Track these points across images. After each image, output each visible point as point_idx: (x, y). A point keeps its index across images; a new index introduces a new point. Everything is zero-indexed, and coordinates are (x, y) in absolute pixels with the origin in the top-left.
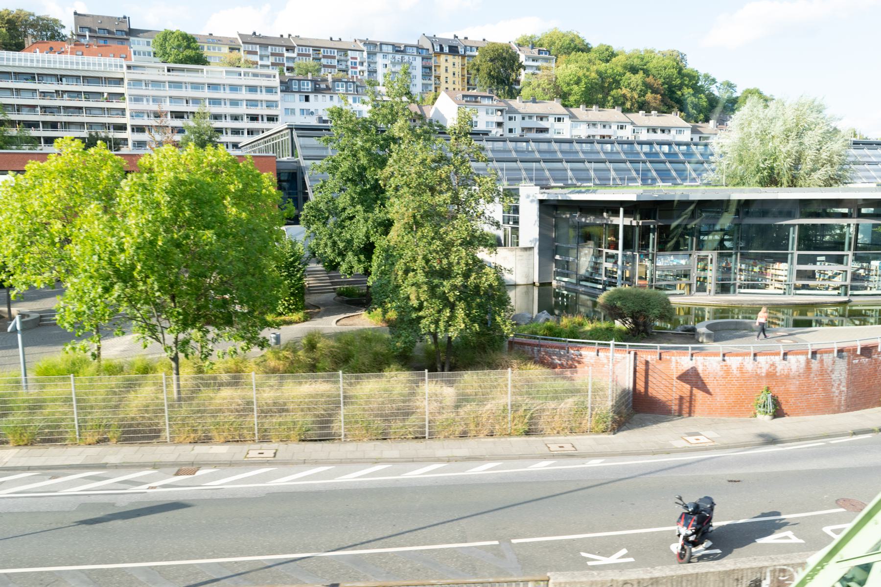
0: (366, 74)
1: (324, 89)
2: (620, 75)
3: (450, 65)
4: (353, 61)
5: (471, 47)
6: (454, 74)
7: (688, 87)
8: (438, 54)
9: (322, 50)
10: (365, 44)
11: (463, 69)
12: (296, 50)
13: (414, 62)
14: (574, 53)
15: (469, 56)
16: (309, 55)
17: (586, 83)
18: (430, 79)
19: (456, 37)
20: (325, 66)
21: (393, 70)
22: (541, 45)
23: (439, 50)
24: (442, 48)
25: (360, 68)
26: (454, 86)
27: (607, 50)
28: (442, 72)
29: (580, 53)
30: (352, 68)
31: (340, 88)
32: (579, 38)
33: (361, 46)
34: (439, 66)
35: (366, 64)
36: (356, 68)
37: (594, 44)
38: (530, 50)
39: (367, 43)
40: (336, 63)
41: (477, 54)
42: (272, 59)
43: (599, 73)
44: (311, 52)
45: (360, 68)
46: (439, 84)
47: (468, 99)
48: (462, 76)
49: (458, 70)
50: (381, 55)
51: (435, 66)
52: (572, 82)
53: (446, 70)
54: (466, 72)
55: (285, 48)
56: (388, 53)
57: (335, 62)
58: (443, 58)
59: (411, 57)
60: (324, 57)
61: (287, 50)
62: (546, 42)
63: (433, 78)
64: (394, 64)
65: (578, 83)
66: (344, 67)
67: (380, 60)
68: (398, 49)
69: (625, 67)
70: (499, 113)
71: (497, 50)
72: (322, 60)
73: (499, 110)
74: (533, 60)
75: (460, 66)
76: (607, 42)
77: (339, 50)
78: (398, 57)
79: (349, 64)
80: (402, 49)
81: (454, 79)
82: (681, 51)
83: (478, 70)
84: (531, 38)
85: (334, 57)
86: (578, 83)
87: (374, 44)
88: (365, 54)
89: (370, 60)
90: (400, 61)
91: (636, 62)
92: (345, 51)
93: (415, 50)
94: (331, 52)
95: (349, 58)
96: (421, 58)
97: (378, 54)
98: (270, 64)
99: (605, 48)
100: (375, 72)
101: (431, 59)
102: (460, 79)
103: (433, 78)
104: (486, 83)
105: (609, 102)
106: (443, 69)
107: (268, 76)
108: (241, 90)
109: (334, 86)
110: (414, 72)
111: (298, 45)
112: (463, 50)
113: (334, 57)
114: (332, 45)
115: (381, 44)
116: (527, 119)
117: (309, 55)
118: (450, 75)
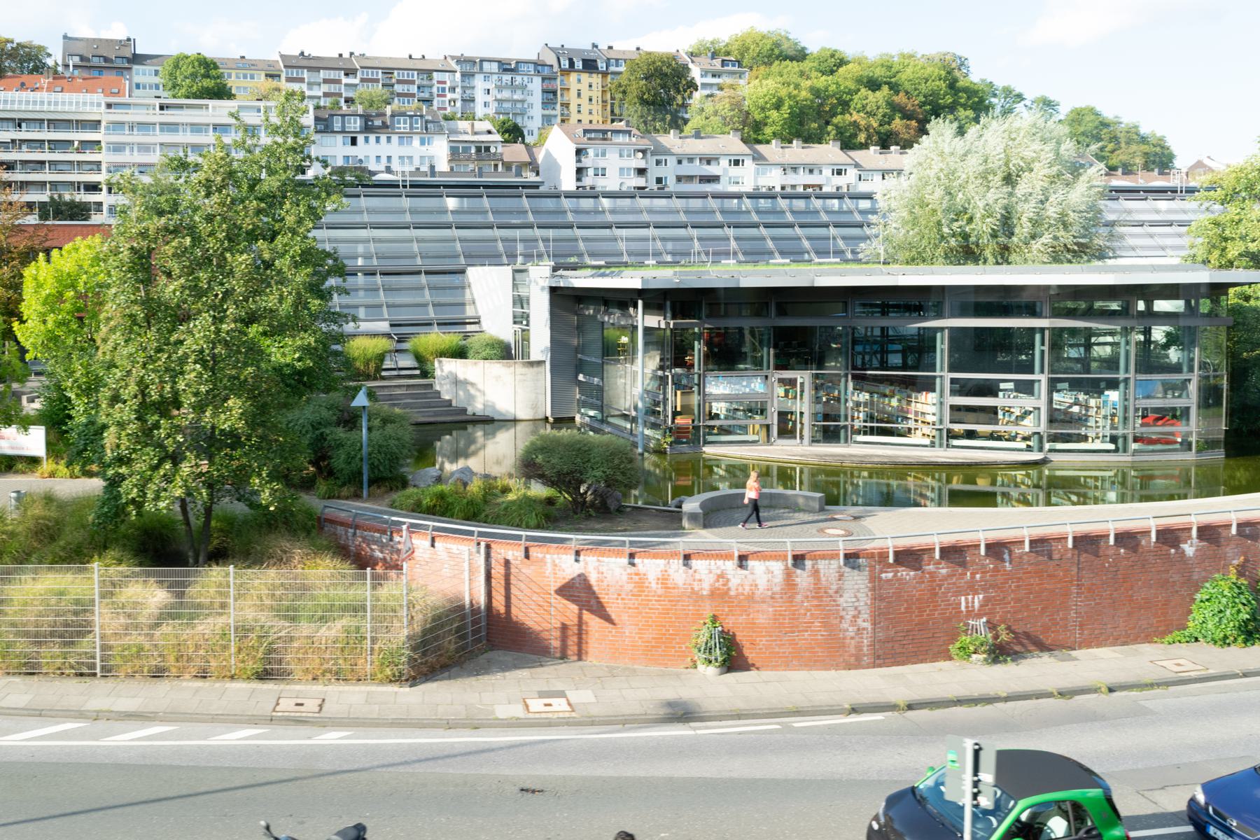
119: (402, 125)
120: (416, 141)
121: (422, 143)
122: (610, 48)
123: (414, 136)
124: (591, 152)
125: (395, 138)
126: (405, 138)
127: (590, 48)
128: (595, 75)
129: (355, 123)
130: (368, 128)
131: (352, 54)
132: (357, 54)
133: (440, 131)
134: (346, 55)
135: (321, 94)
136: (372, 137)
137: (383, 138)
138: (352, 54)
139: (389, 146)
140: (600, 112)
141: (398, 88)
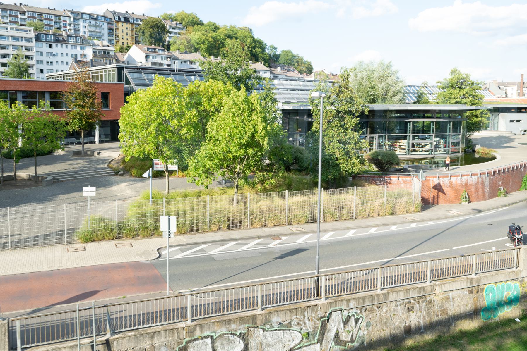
0: (73, 31)
1: (62, 41)
2: (224, 40)
3: (125, 29)
4: (64, 23)
5: (137, 19)
6: (127, 34)
7: (258, 47)
8: (117, 22)
9: (44, 15)
10: (71, 13)
11: (132, 31)
12: (26, 14)
13: (103, 26)
14: (196, 26)
15: (136, 24)
16: (35, 18)
17: (207, 44)
18: (112, 37)
19: (127, 12)
20: (46, 25)
21: (90, 30)
22: (176, 20)
23: (118, 19)
24: (119, 18)
25: (68, 27)
26: (127, 41)
27: (213, 25)
28: (120, 32)
29: (199, 26)
30: (64, 27)
31: (72, 40)
32: (196, 17)
33: (69, 14)
34: (118, 29)
35: (72, 25)
36: (66, 27)
37: (205, 22)
38: (171, 22)
39: (73, 13)
40: (53, 24)
41: (141, 23)
42: (10, 19)
43: (213, 38)
44: (37, 16)
45: (68, 27)
46: (118, 40)
47: (151, 50)
48: (132, 35)
49: (129, 32)
50: (82, 20)
51: (116, 29)
52: (200, 42)
53: (123, 32)
54: (134, 33)
55: (19, 12)
56: (87, 19)
57: (52, 23)
58: (120, 24)
59: (101, 23)
60: (45, 19)
61: (20, 14)
62: (179, 18)
63: (114, 36)
64: (90, 26)
65: (203, 43)
66: (58, 26)
67: (81, 23)
68: (92, 17)
69: (226, 35)
70: (169, 59)
71: (155, 22)
72: (44, 21)
73: (168, 58)
74: (173, 29)
75: (131, 30)
76: (213, 20)
77: (55, 16)
78: (93, 22)
79: (62, 24)
80: (95, 17)
81: (127, 37)
82: (250, 28)
83: (143, 33)
84: (169, 15)
85: (52, 20)
86: (203, 43)
87: (77, 14)
88: (72, 19)
89: (75, 23)
90: (94, 24)
91: (231, 33)
92: (59, 17)
93: (103, 18)
94: (50, 16)
95: (62, 21)
96: (107, 24)
97: (80, 20)
98: (9, 22)
99: (212, 24)
100: (79, 30)
101: (113, 24)
102: (131, 37)
103: (114, 36)
104: (149, 41)
105: (220, 54)
106: (120, 31)
107: (26, 31)
108: (8, 39)
109: (68, 39)
110: (103, 32)
111: (28, 11)
112: (132, 20)
113: (52, 20)
114: (49, 12)
115: (82, 13)
116: (183, 63)
117: (35, 18)
118: (125, 34)
119: (72, 40)
120: (78, 48)
121: (81, 49)
122: (133, 13)
123: (78, 46)
124: (151, 57)
125: (69, 46)
126: (74, 46)
127: (125, 12)
128: (128, 24)
129: (51, 38)
130: (57, 41)
131: (21, 4)
132: (23, 4)
133: (89, 44)
134: (18, 4)
135: (8, 21)
136: (59, 45)
137: (64, 45)
138: (21, 4)
139: (67, 49)
140: (131, 40)
141: (45, 22)
